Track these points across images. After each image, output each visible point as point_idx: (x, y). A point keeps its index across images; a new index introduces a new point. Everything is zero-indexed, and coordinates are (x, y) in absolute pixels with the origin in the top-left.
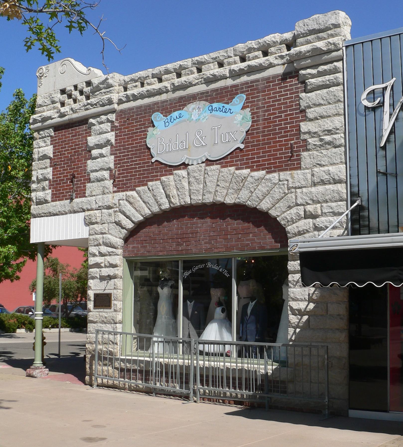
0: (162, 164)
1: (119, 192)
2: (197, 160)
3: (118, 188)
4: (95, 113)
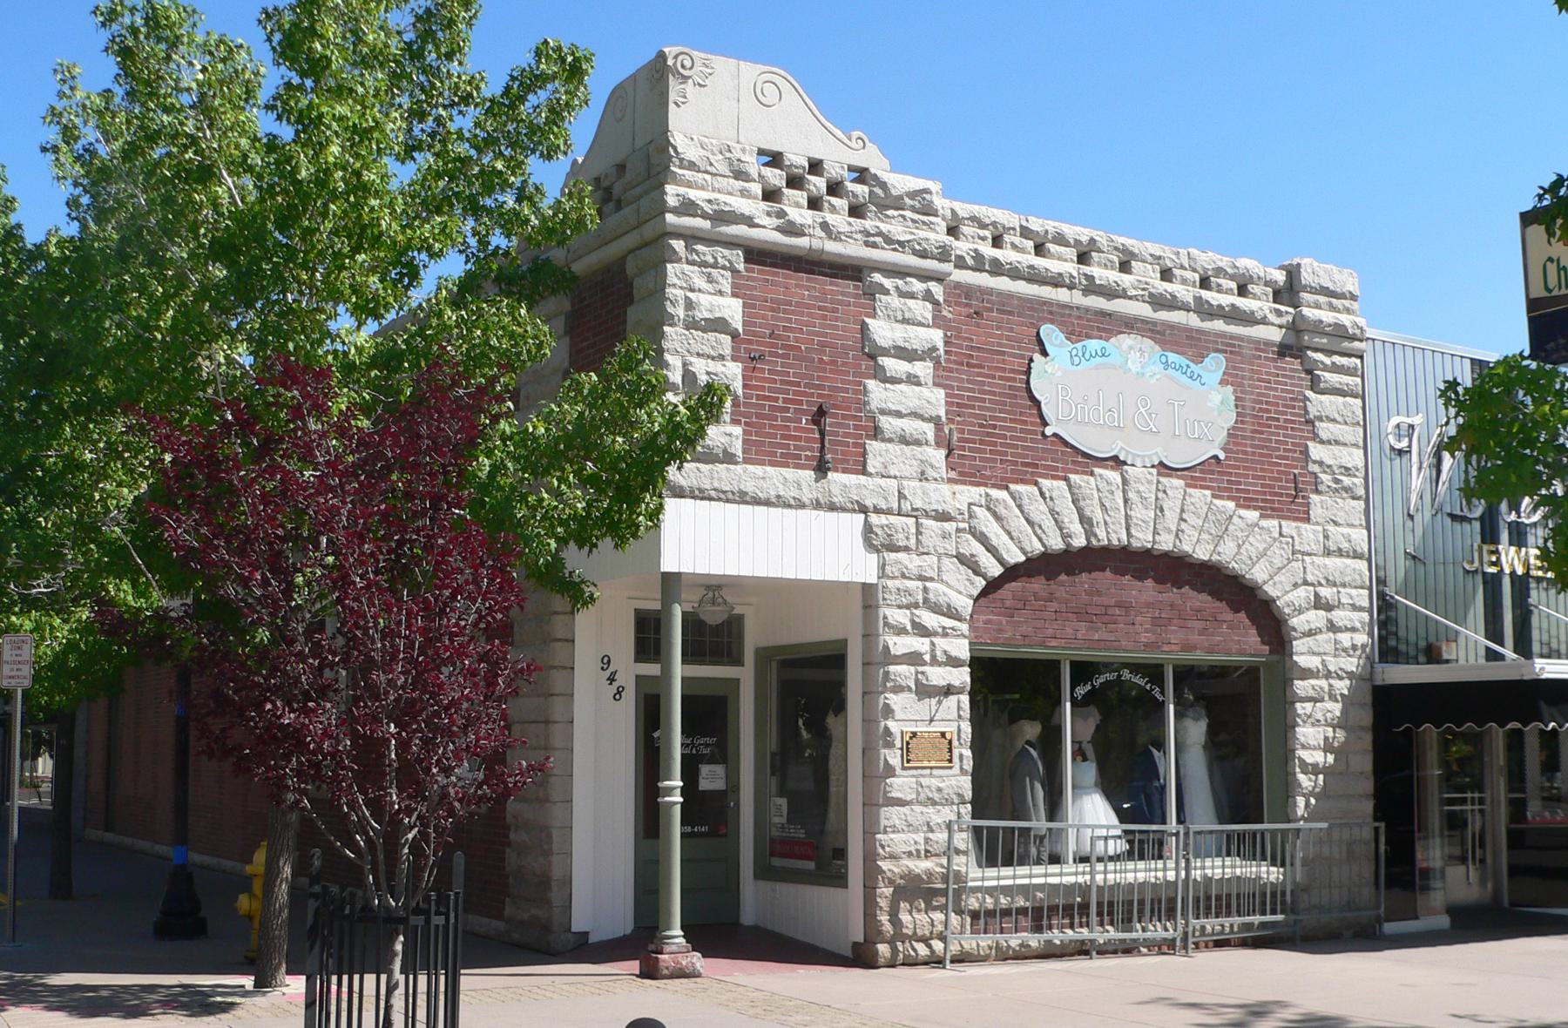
0: (1066, 443)
1: (964, 483)
2: (1143, 457)
3: (961, 474)
4: (896, 265)
